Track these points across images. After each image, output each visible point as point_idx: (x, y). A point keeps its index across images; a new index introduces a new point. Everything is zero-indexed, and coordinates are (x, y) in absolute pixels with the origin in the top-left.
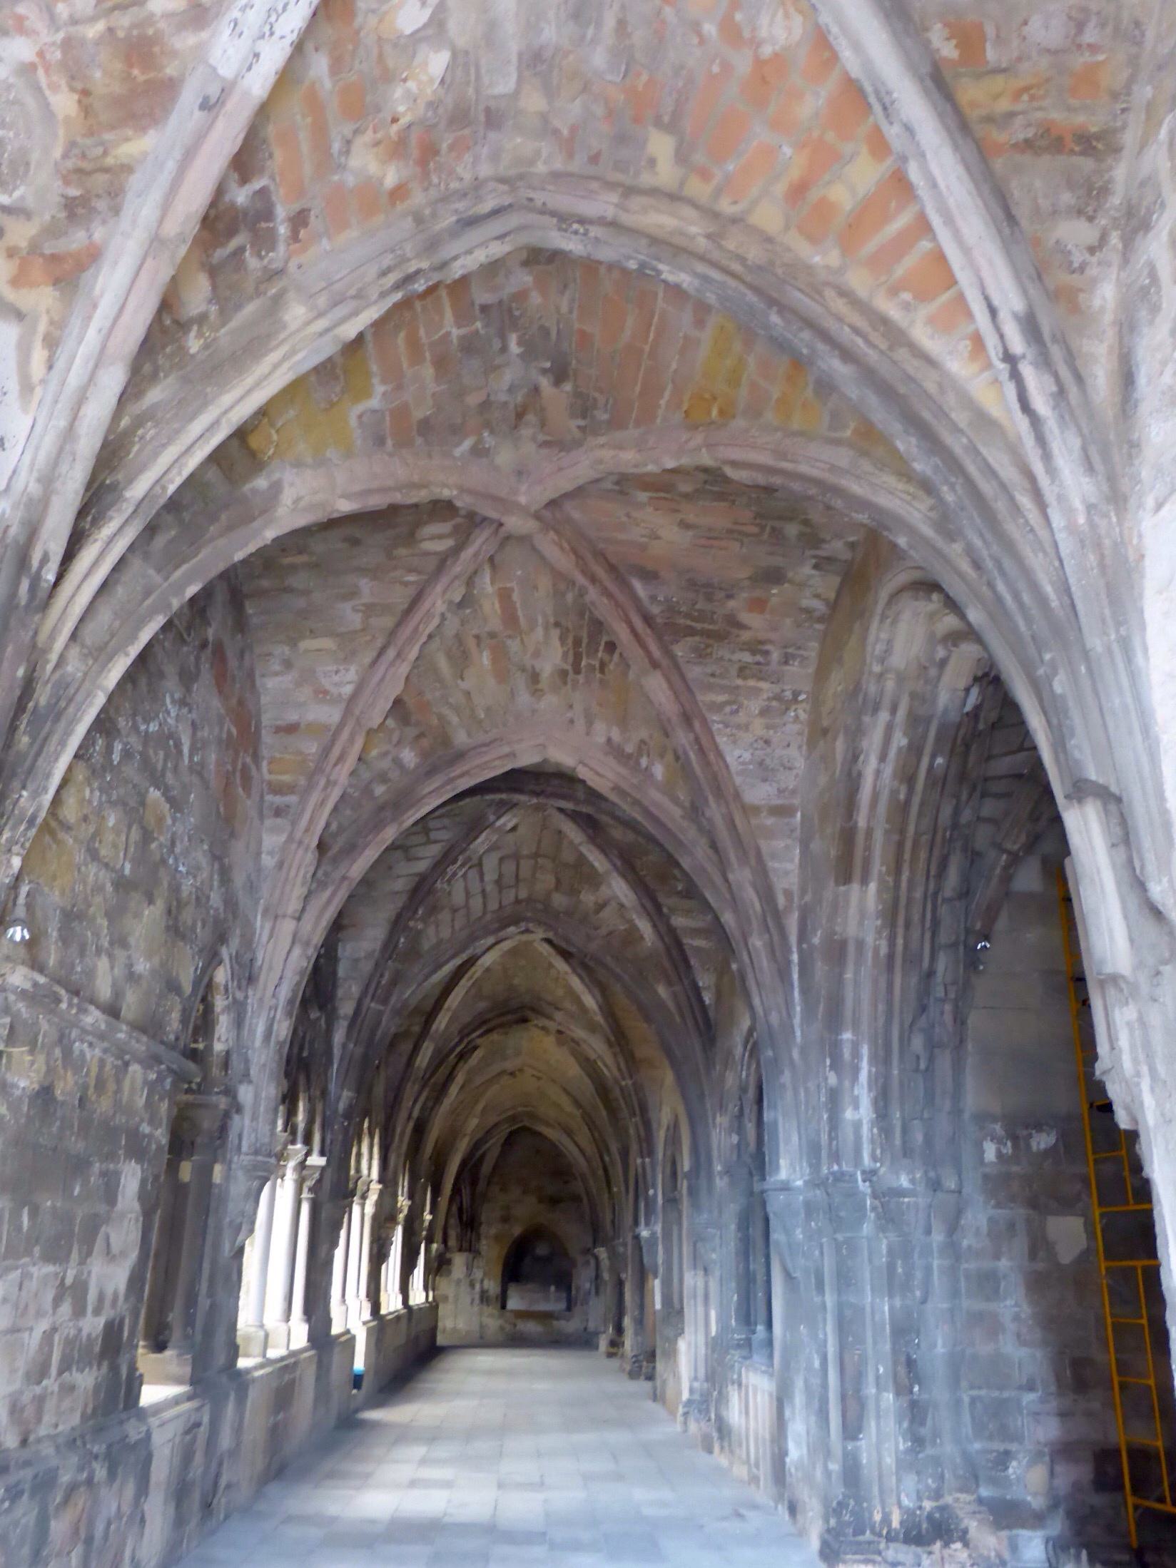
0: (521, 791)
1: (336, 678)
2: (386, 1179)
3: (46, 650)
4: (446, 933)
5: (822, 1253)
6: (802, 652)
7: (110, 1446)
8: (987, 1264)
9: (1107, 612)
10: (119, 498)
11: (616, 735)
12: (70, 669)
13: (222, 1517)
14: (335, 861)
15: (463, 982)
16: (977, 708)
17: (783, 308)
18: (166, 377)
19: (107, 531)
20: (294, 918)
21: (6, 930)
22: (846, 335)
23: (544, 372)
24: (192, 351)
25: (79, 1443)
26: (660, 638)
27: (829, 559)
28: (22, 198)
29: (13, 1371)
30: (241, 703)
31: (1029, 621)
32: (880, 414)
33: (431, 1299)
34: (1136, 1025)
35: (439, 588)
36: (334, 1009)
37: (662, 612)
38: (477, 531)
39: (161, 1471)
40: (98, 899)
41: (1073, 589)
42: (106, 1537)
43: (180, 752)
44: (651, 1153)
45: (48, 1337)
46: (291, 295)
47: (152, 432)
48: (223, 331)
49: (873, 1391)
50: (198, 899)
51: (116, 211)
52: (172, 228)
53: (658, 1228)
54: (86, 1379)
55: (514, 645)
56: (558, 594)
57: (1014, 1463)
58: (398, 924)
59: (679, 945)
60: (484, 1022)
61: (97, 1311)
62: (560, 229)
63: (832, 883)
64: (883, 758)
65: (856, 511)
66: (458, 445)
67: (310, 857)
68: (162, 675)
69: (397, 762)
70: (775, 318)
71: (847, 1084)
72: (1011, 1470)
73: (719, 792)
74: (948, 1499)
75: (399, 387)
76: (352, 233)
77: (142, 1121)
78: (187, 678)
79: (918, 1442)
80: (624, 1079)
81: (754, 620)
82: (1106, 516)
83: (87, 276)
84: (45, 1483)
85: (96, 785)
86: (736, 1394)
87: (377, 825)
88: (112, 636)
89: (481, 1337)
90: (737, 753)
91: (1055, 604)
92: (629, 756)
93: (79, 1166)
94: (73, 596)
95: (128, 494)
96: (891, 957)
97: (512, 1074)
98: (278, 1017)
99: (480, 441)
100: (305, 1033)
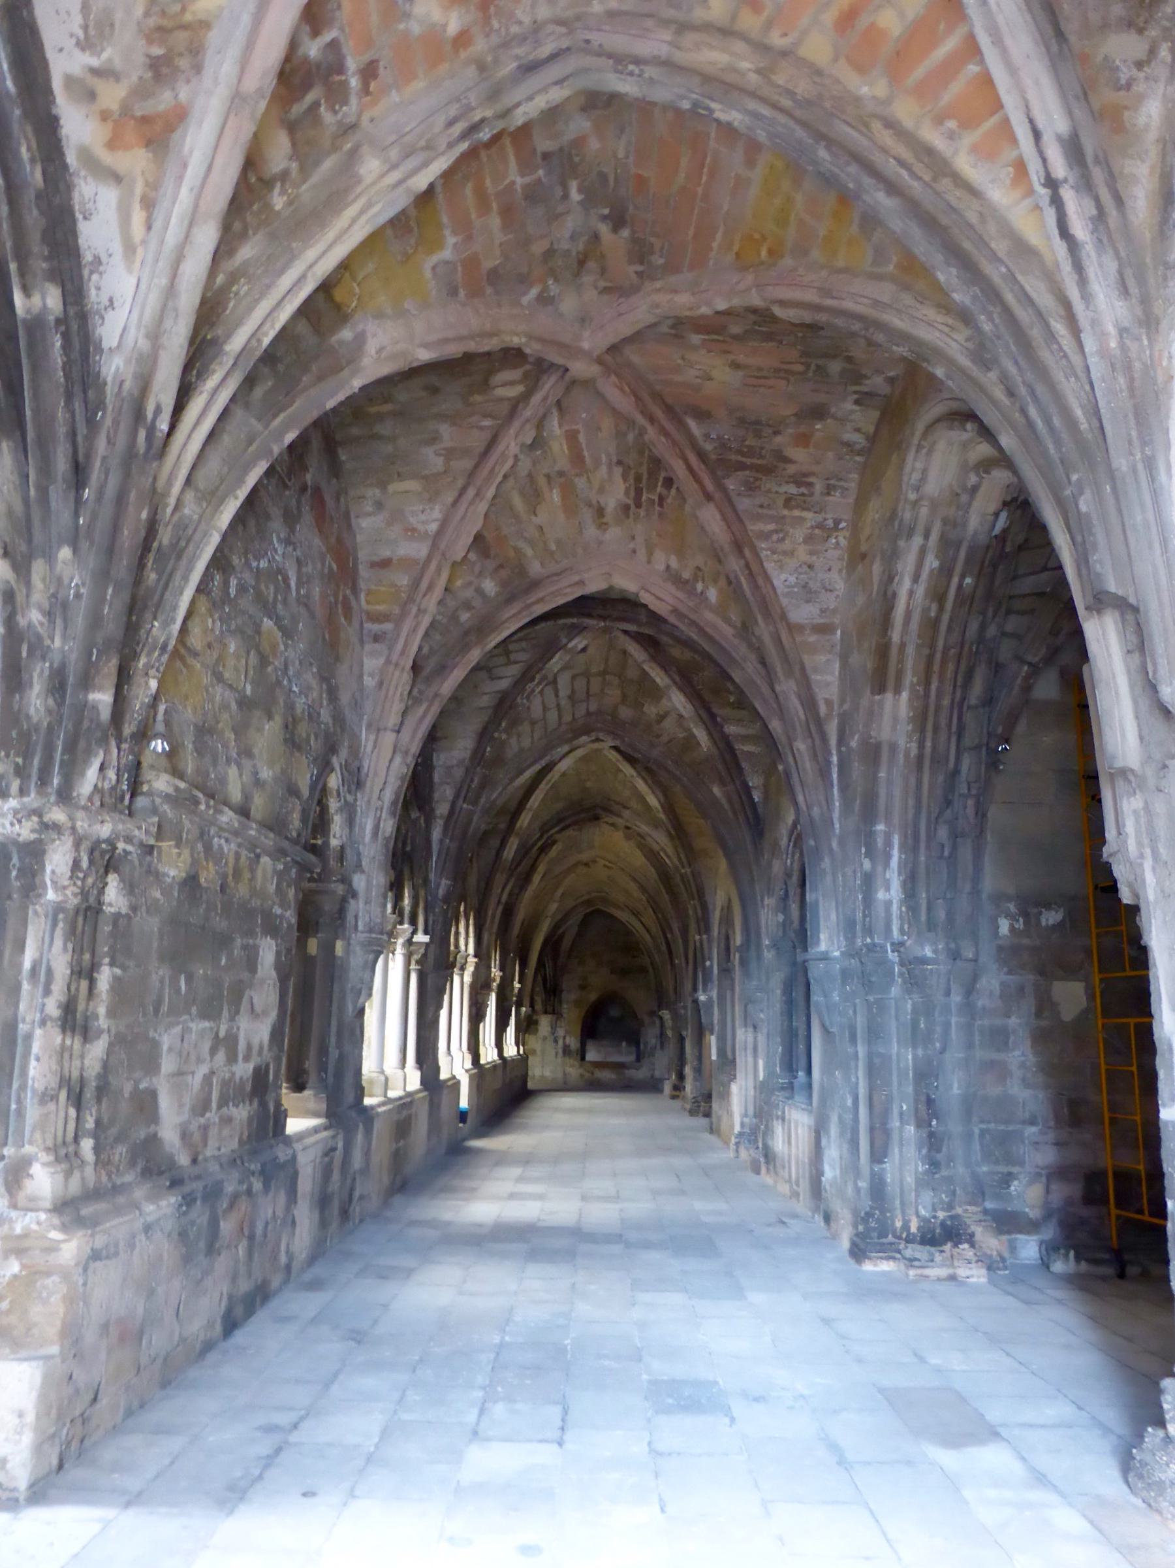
0: (590, 616)
1: (423, 517)
2: (481, 953)
3: (166, 494)
4: (526, 742)
5: (855, 1012)
6: (842, 483)
7: (263, 1165)
8: (998, 1022)
9: (1134, 433)
10: (220, 352)
11: (674, 563)
12: (187, 511)
13: (357, 1221)
14: (428, 680)
15: (542, 786)
16: (1005, 531)
17: (830, 142)
18: (254, 234)
19: (211, 383)
20: (393, 730)
21: (149, 743)
22: (891, 168)
23: (604, 218)
24: (278, 207)
25: (238, 1162)
26: (713, 473)
27: (870, 394)
28: (110, 60)
29: (181, 1106)
30: (339, 540)
31: (1058, 442)
32: (923, 247)
34: (1142, 813)
35: (512, 431)
36: (432, 810)
37: (715, 448)
38: (545, 377)
39: (306, 1184)
40: (225, 716)
41: (1102, 411)
42: (265, 1236)
43: (288, 586)
44: (708, 930)
45: (207, 1079)
46: (365, 149)
47: (246, 288)
48: (304, 187)
49: (898, 1124)
50: (310, 715)
51: (198, 68)
52: (251, 84)
53: (714, 994)
54: (241, 1113)
55: (581, 483)
56: (620, 435)
57: (1016, 1183)
58: (484, 735)
59: (732, 751)
61: (247, 1058)
62: (617, 71)
63: (868, 692)
64: (916, 579)
65: (898, 345)
66: (525, 293)
67: (407, 677)
68: (268, 517)
69: (480, 591)
70: (823, 153)
71: (880, 869)
72: (1012, 1188)
73: (767, 614)
74: (959, 1210)
75: (469, 238)
76: (419, 84)
77: (274, 903)
78: (291, 519)
79: (934, 1165)
80: (683, 867)
81: (800, 455)
82: (1138, 339)
83: (176, 136)
84: (212, 1194)
85: (216, 616)
86: (780, 1128)
87: (465, 648)
88: (222, 481)
89: (565, 1083)
90: (783, 577)
91: (1084, 426)
92: (687, 582)
93: (224, 941)
94: (185, 445)
95: (227, 348)
96: (920, 758)
97: (586, 865)
98: (384, 815)
99: (545, 289)
100: (407, 832)
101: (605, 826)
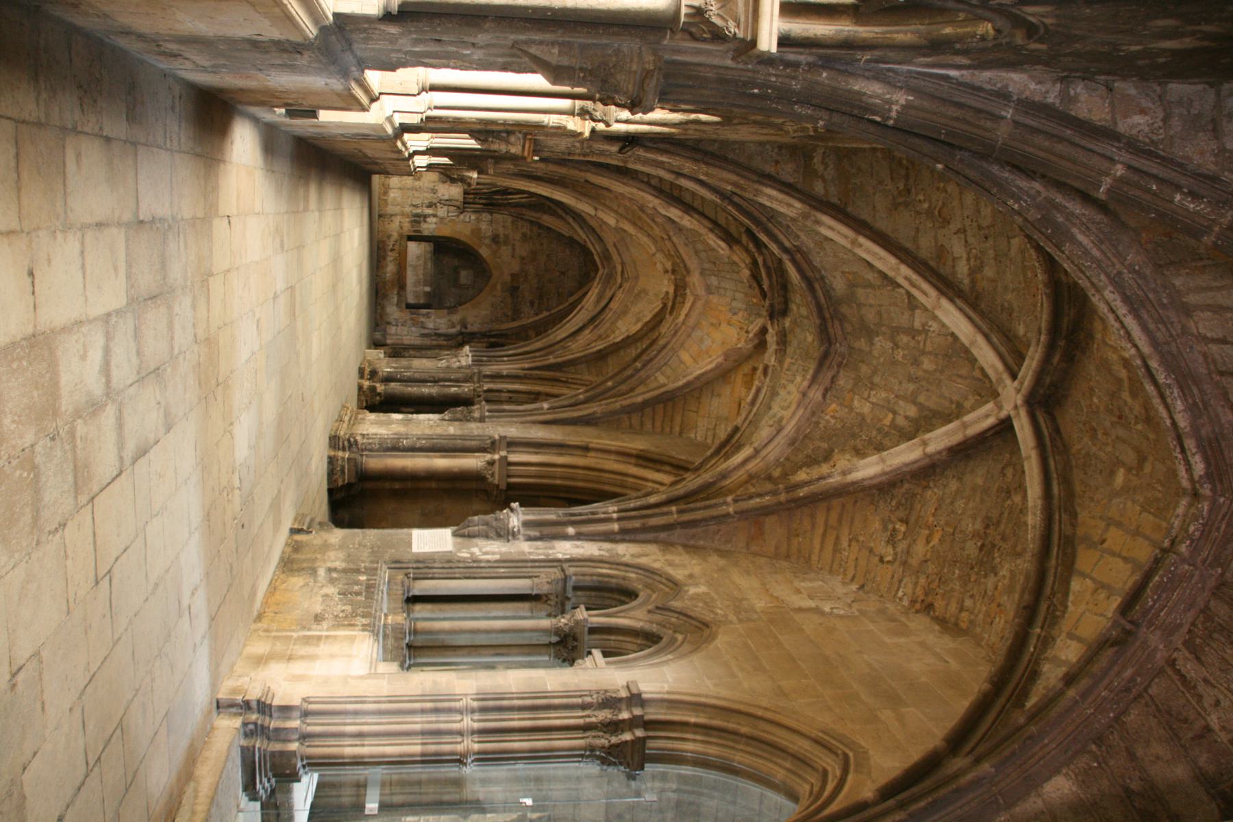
15: (905, 270)
36: (1087, 76)
44: (625, 535)
80: (736, 501)
89: (380, 216)
101: (759, 322)
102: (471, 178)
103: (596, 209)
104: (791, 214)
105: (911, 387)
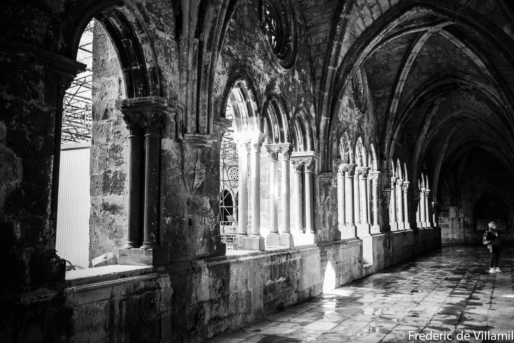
15: (406, 65)
33: (435, 225)
60: (426, 87)
80: (506, 105)
101: (462, 92)
102: (434, 204)
103: (442, 152)
104: (398, 102)
105: (450, 51)
